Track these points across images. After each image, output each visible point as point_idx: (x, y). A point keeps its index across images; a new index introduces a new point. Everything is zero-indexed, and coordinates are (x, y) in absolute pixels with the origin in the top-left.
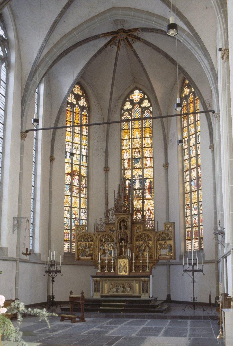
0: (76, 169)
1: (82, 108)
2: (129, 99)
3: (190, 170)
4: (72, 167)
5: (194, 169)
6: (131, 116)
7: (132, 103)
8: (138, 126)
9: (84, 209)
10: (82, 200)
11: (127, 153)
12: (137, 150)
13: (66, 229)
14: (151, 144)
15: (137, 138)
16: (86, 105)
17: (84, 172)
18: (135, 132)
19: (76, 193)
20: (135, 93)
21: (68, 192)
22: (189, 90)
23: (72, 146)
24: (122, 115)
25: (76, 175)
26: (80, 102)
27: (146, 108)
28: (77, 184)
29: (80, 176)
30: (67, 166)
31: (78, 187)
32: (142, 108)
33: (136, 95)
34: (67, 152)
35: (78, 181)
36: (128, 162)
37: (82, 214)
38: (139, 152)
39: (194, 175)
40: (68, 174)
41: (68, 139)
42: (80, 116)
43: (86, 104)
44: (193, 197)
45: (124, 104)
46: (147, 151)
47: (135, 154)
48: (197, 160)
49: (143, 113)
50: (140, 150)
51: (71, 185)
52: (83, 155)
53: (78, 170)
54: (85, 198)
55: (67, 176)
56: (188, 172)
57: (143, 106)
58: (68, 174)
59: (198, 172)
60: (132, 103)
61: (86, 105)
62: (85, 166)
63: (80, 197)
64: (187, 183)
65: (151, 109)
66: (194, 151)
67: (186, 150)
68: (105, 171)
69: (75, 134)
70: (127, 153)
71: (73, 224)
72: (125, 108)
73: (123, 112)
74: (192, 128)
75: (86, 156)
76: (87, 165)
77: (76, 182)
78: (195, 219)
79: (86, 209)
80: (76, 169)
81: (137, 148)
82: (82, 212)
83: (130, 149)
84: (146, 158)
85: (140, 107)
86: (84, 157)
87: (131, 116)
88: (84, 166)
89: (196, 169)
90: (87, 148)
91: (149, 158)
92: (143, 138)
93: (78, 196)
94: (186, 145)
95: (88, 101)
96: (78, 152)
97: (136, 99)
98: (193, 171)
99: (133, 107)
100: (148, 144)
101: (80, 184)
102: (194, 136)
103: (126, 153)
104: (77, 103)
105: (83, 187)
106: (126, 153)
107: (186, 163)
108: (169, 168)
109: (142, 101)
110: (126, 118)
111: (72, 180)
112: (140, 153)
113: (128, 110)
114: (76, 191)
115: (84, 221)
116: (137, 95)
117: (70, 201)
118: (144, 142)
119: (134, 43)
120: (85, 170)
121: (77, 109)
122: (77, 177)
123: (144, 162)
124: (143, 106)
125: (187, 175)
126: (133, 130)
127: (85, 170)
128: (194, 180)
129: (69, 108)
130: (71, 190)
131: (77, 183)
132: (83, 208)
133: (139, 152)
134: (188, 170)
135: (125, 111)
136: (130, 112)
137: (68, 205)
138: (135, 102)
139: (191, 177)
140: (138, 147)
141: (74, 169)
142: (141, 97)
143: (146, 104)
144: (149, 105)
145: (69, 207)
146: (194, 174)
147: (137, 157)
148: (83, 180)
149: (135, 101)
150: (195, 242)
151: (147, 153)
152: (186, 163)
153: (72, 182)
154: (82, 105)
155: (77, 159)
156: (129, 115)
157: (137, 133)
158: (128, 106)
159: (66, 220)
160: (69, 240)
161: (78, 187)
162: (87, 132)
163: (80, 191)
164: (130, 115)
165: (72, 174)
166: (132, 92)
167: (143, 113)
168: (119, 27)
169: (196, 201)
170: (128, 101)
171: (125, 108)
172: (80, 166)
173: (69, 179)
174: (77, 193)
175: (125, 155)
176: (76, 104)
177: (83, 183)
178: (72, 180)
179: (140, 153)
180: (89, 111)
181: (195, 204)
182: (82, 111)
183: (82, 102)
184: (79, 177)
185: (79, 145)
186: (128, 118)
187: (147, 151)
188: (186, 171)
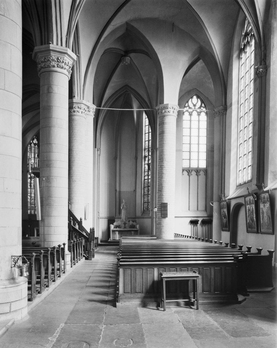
1: (35, 144)
21: (29, 187)
40: (29, 178)
43: (37, 142)
51: (31, 183)
61: (37, 142)
71: (32, 202)
95: (38, 140)
104: (33, 142)
111: (31, 180)
114: (33, 186)
117: (30, 191)
121: (33, 145)
130: (31, 186)
153: (31, 182)
154: (35, 143)
159: (28, 200)
176: (32, 143)
178: (31, 180)
182: (35, 146)
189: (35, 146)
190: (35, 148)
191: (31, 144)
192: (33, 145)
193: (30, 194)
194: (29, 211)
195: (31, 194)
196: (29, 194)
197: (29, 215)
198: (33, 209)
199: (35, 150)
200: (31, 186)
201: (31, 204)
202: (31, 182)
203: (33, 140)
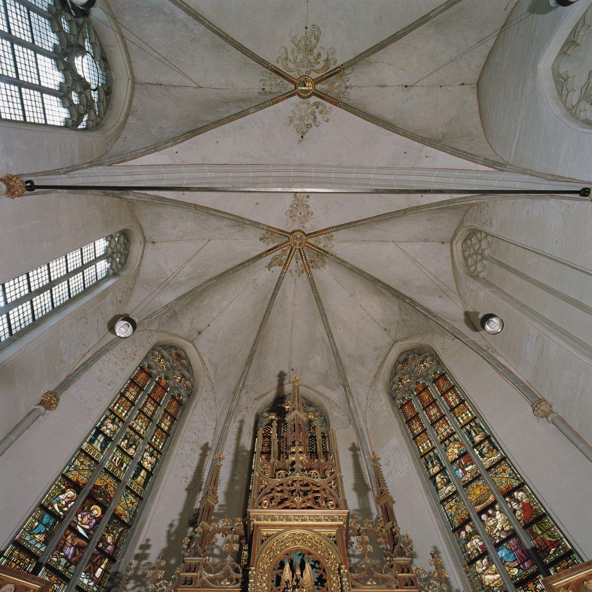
0: (106, 486)
19: (66, 557)
30: (82, 463)
34: (103, 433)
35: (94, 521)
39: (499, 527)
41: (120, 411)
55: (67, 487)
64: (478, 562)
69: (139, 413)
74: (440, 429)
80: (106, 486)
94: (433, 466)
98: (489, 515)
107: (451, 507)
110: (267, 435)
119: (313, 267)
120: (132, 503)
127: (132, 503)
131: (87, 527)
148: (113, 529)
152: (451, 507)
161: (83, 542)
168: (296, 227)
173: (67, 500)
174: (68, 561)
184: (103, 513)
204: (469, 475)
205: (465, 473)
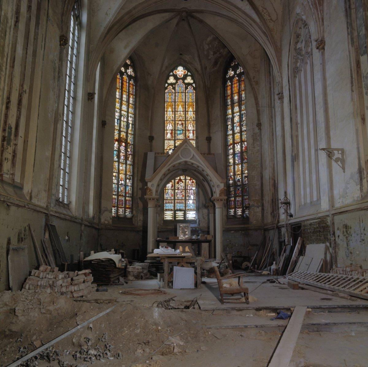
1: (130, 77)
2: (173, 73)
3: (234, 143)
4: (119, 134)
5: (238, 144)
6: (175, 90)
7: (176, 77)
8: (181, 100)
9: (130, 175)
10: (128, 166)
11: (171, 125)
12: (180, 123)
13: (114, 195)
14: (194, 118)
15: (180, 111)
16: (133, 74)
17: (130, 139)
18: (178, 105)
20: (179, 69)
21: (115, 158)
22: (233, 73)
23: (120, 113)
24: (166, 88)
25: (123, 142)
26: (128, 71)
27: (189, 84)
28: (124, 151)
29: (127, 143)
31: (124, 154)
32: (186, 84)
33: (180, 71)
36: (171, 133)
37: (128, 181)
38: (182, 124)
39: (238, 150)
40: (117, 140)
42: (128, 85)
44: (236, 169)
45: (168, 78)
46: (190, 125)
47: (178, 126)
48: (241, 136)
49: (186, 88)
50: (183, 122)
51: (119, 151)
52: (130, 123)
53: (125, 137)
54: (131, 165)
56: (231, 146)
57: (186, 81)
58: (117, 140)
59: (242, 147)
60: (176, 77)
61: (133, 74)
62: (131, 134)
63: (126, 164)
65: (194, 85)
66: (238, 128)
67: (229, 126)
68: (149, 139)
70: (171, 125)
71: (120, 190)
72: (169, 82)
73: (166, 85)
75: (132, 124)
76: (133, 133)
77: (122, 148)
78: (239, 189)
79: (131, 175)
81: (180, 120)
82: (128, 179)
83: (173, 121)
84: (188, 130)
85: (184, 82)
86: (131, 125)
87: (175, 90)
88: (130, 134)
89: (240, 144)
90: (133, 116)
91: (192, 131)
92: (186, 112)
93: (124, 163)
96: (125, 120)
97: (180, 75)
99: (177, 82)
100: (191, 118)
101: (126, 150)
102: (238, 114)
103: (170, 124)
104: (126, 72)
105: (129, 154)
106: (170, 124)
108: (212, 141)
109: (185, 77)
111: (120, 145)
112: (183, 126)
113: (172, 84)
115: (129, 187)
116: (180, 71)
118: (187, 116)
121: (125, 77)
122: (124, 144)
123: (187, 134)
124: (186, 81)
125: (230, 149)
126: (176, 103)
128: (238, 153)
129: (118, 76)
132: (128, 174)
133: (182, 124)
134: (231, 144)
135: (169, 84)
136: (174, 86)
137: (115, 171)
138: (179, 77)
139: (234, 151)
140: (182, 119)
141: (121, 136)
142: (185, 73)
143: (189, 80)
144: (192, 82)
145: (116, 173)
146: (238, 148)
147: (180, 129)
149: (179, 76)
150: (238, 211)
151: (189, 126)
153: (119, 148)
155: (124, 126)
156: (172, 89)
157: (180, 107)
158: (172, 80)
159: (114, 186)
160: (116, 205)
162: (133, 101)
163: (126, 158)
164: (174, 88)
165: (120, 141)
166: (176, 68)
167: (186, 88)
169: (239, 173)
170: (171, 75)
171: (169, 82)
172: (127, 133)
175: (168, 126)
177: (129, 150)
178: (120, 145)
179: (183, 126)
180: (135, 81)
181: (238, 176)
182: (130, 80)
183: (130, 71)
185: (126, 113)
186: (172, 91)
187: (190, 125)
188: (230, 145)
189: (130, 80)
190: (129, 83)
191: (122, 74)
192: (125, 77)
193: (117, 174)
194: (114, 210)
195: (119, 173)
196: (114, 174)
197: (114, 217)
198: (122, 205)
199: (129, 87)
200: (119, 157)
201: (118, 195)
202: (119, 148)
203: (126, 67)
204: (237, 130)
205: (236, 129)
